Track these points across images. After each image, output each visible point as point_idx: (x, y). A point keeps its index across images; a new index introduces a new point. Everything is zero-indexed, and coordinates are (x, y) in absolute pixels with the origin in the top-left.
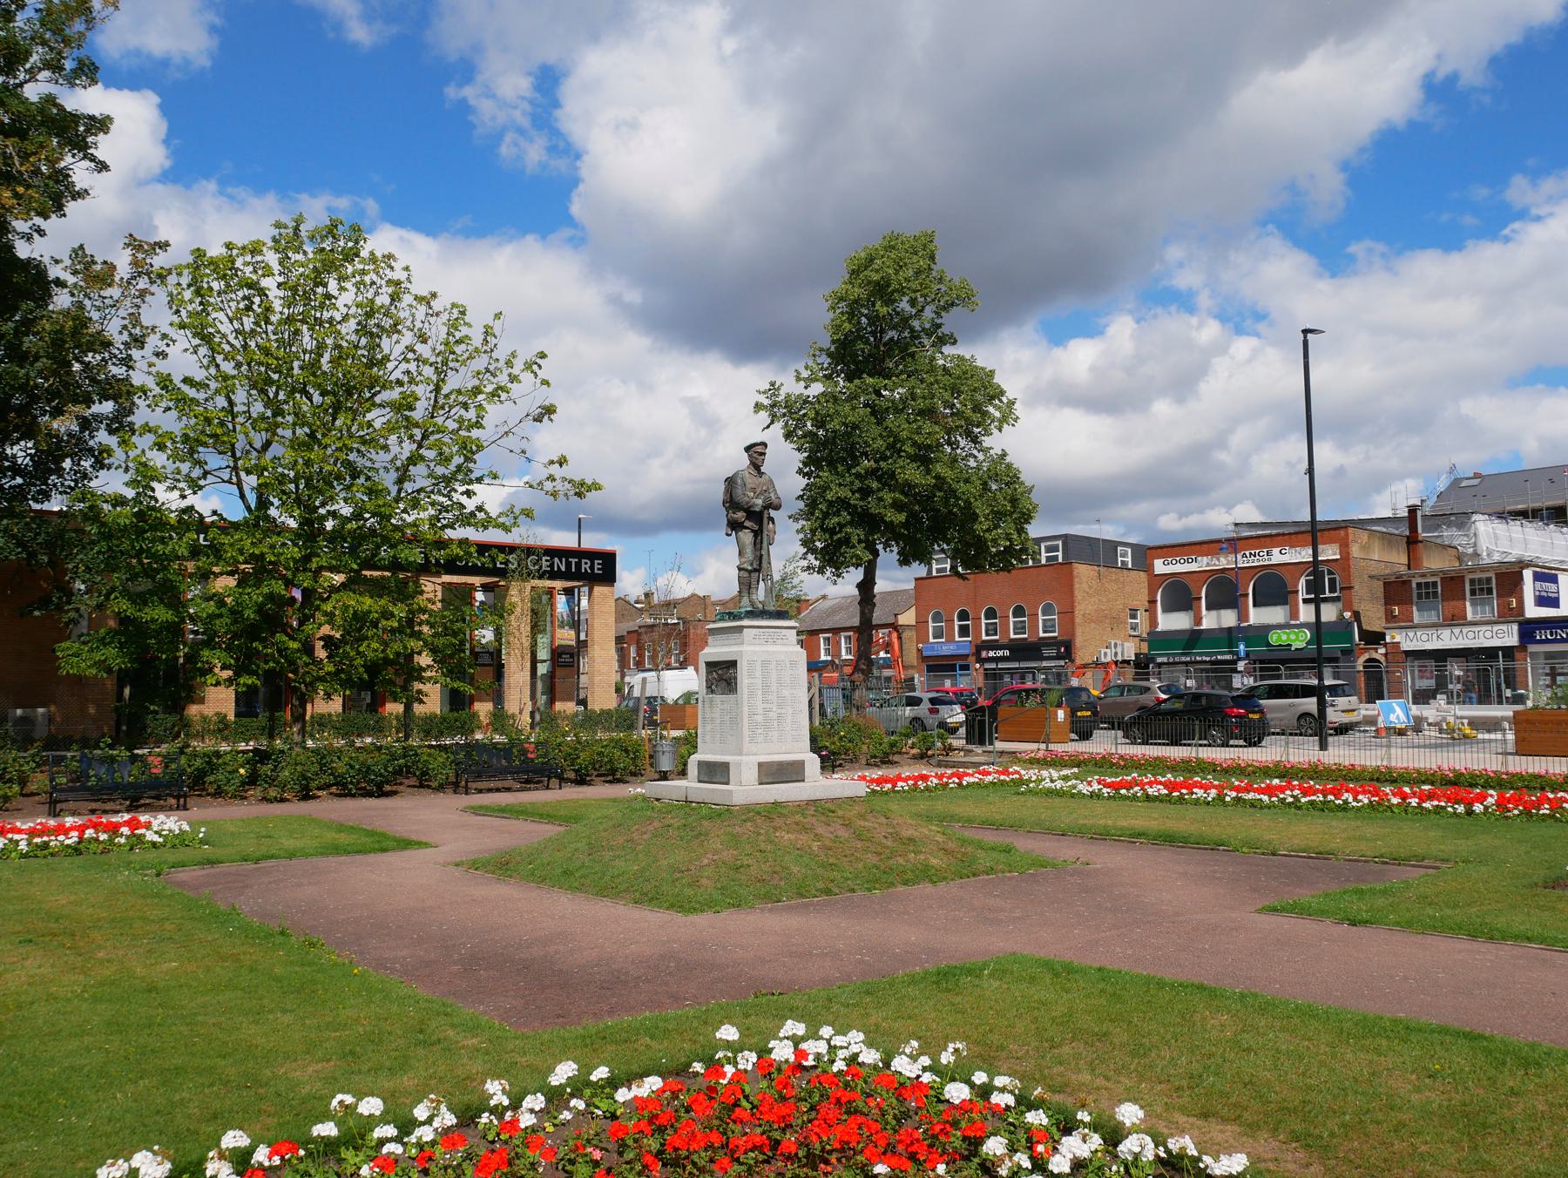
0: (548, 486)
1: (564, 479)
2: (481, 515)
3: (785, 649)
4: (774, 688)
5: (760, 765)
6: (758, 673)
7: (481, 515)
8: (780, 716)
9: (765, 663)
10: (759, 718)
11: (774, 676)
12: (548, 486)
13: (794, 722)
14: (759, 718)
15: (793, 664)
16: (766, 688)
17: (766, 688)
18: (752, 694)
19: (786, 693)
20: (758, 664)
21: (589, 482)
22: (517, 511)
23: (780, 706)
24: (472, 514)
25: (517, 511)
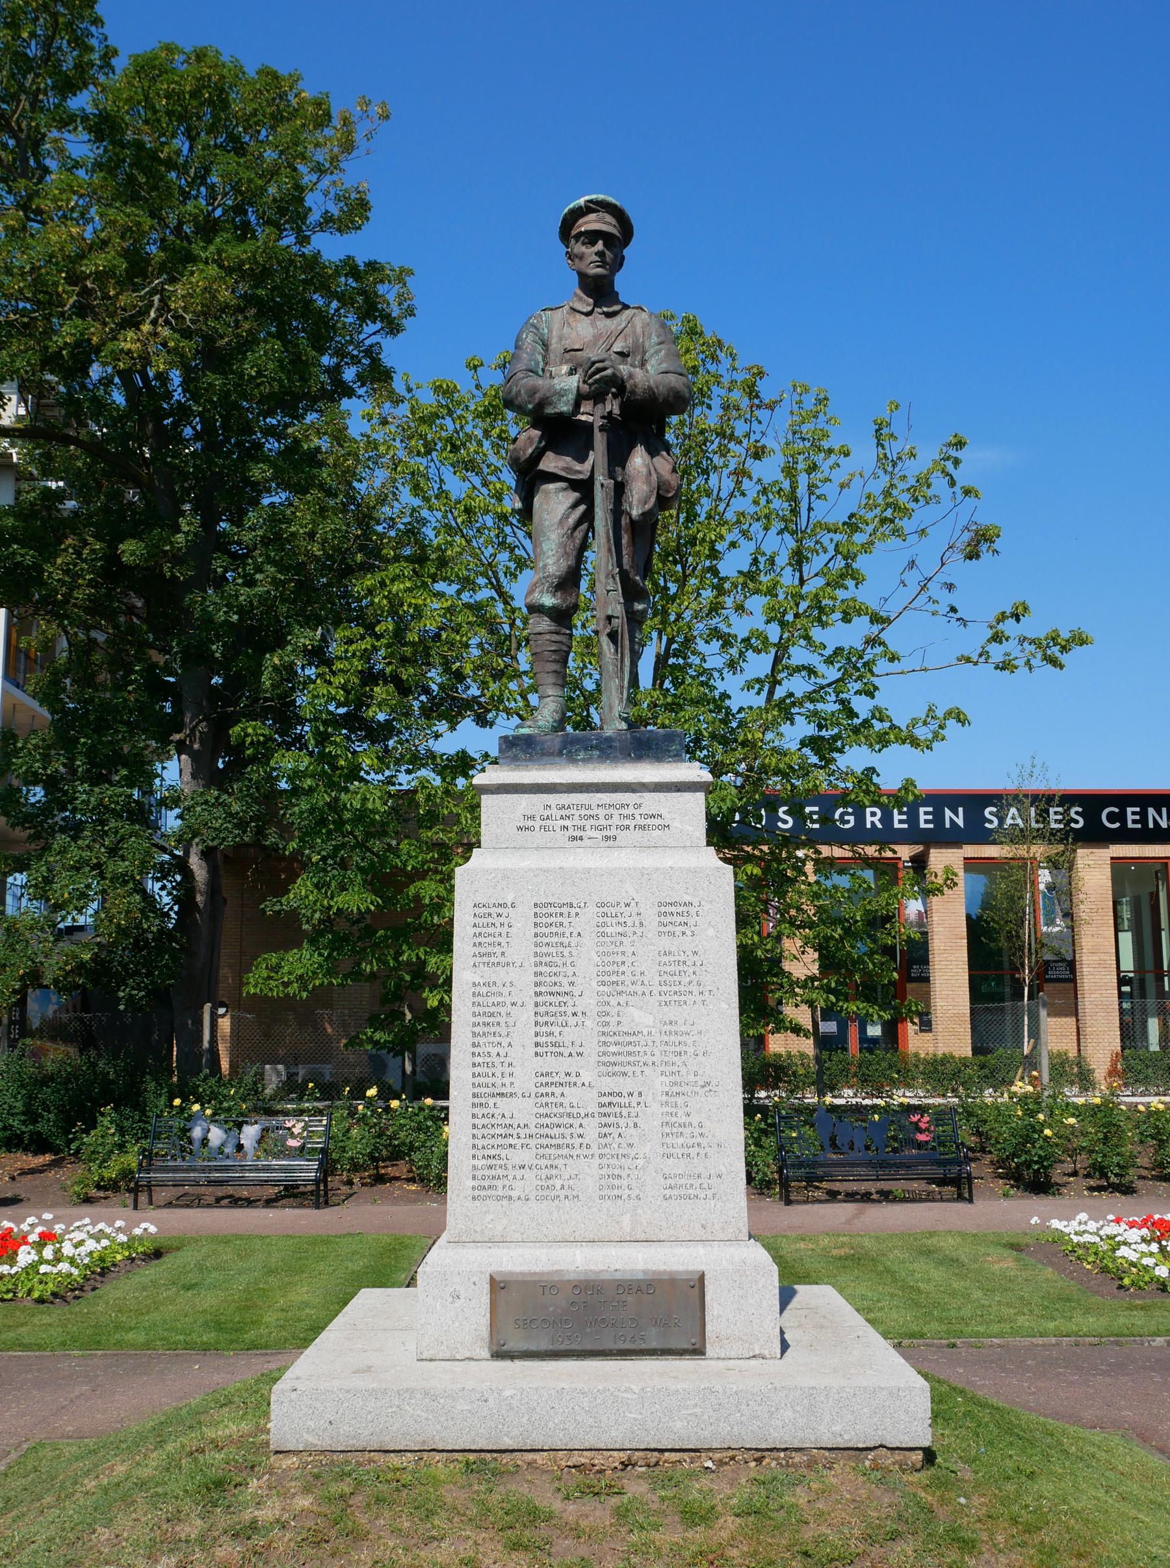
0: (997, 652)
1: (1022, 640)
2: (878, 726)
3: (648, 861)
4: (589, 1003)
5: (498, 1286)
6: (520, 945)
7: (878, 726)
8: (609, 1104)
9: (551, 916)
10: (522, 1110)
11: (586, 961)
12: (997, 652)
13: (672, 1128)
14: (522, 1110)
15: (675, 914)
16: (552, 999)
17: (552, 999)
18: (488, 1021)
19: (641, 1017)
20: (522, 923)
21: (1065, 635)
22: (940, 713)
23: (610, 1066)
24: (866, 723)
25: (940, 713)
